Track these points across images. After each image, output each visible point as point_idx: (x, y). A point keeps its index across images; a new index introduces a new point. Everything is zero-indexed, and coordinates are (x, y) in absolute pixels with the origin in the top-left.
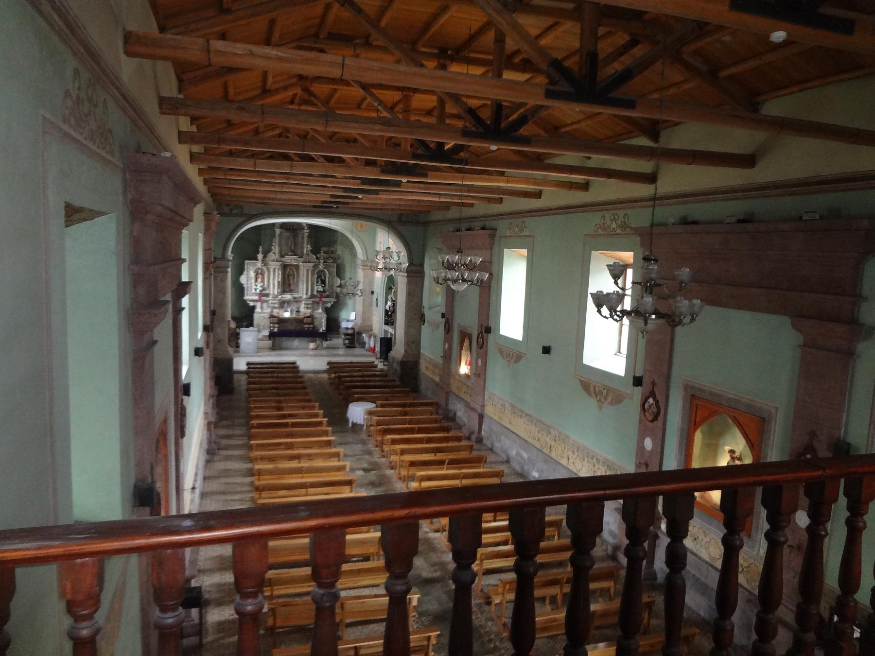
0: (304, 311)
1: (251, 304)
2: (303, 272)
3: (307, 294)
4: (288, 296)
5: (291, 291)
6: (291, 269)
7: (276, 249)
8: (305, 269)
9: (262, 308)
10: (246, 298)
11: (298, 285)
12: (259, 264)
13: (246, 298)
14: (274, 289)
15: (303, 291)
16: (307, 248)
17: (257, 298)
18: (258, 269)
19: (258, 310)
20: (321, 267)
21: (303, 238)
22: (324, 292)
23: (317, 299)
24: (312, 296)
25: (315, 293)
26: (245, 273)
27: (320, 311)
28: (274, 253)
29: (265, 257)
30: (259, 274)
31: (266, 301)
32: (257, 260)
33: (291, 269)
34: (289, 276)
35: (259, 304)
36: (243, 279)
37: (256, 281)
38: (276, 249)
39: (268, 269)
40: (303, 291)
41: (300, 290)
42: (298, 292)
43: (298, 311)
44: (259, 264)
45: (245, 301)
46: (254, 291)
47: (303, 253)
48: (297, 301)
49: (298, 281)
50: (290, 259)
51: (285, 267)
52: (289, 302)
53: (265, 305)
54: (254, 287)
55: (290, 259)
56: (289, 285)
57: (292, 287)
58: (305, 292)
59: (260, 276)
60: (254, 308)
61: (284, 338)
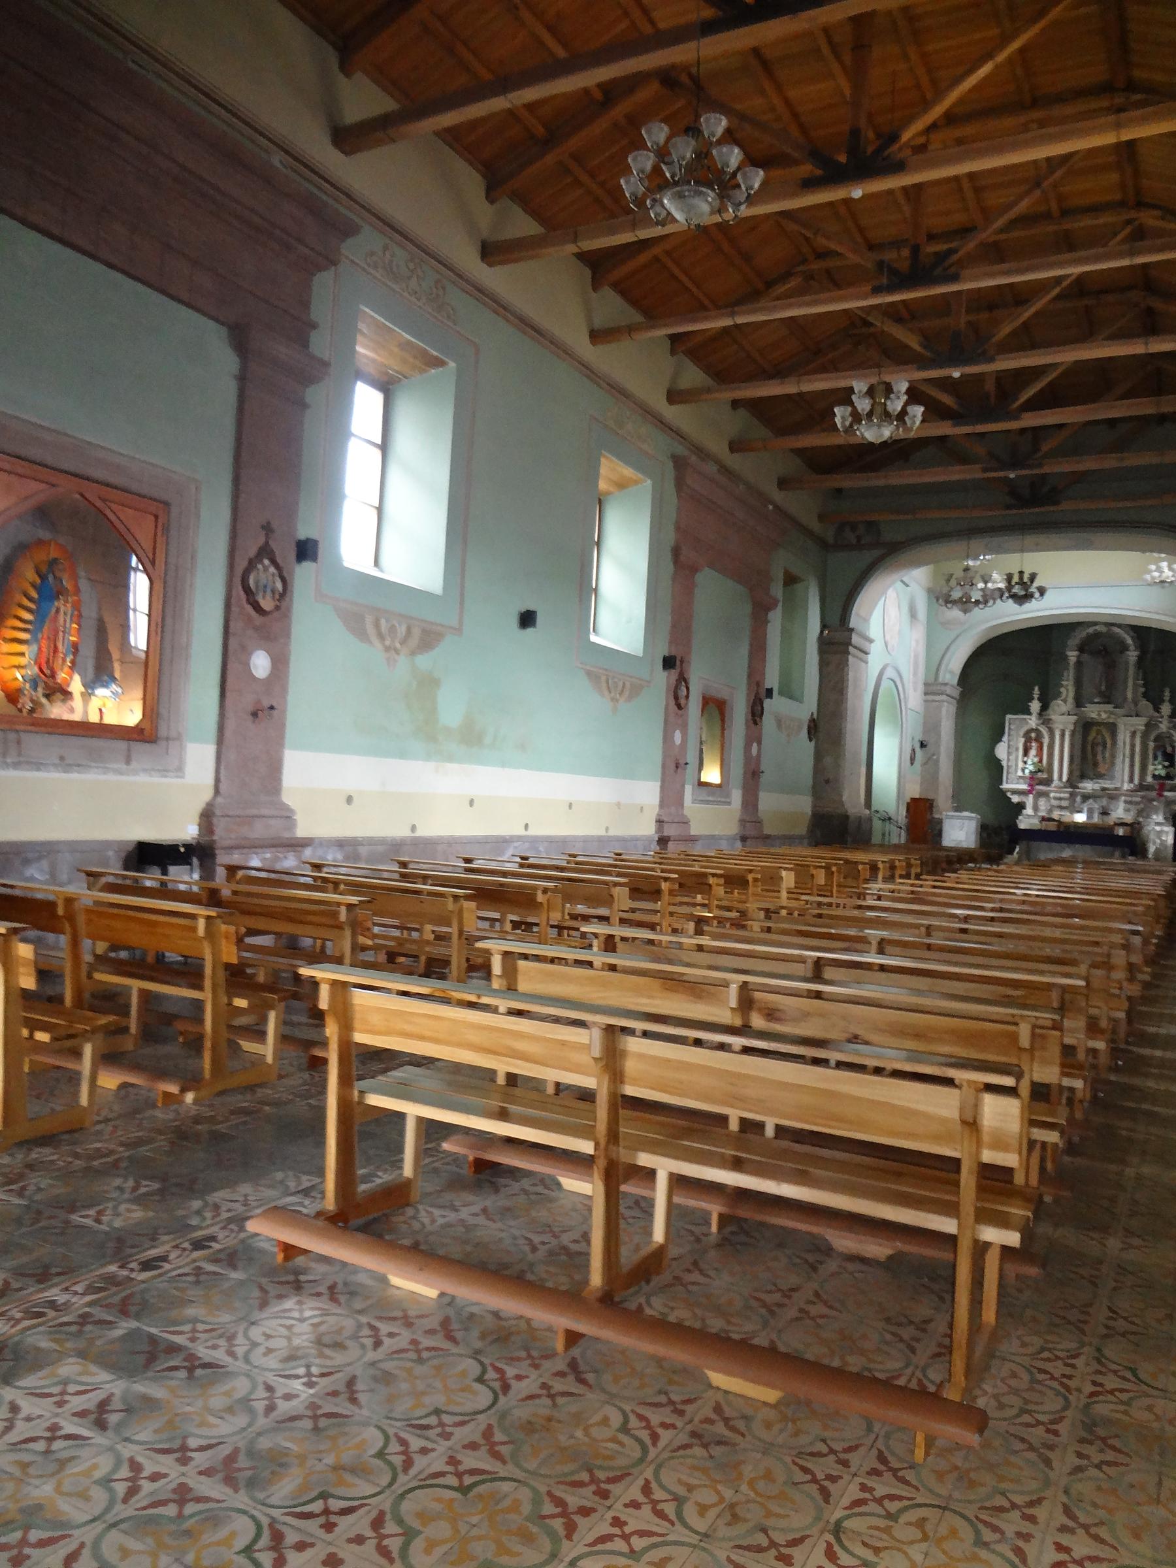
0: (1120, 812)
1: (1015, 799)
2: (1123, 737)
3: (1131, 780)
4: (1088, 786)
5: (1099, 776)
6: (1099, 732)
7: (1068, 689)
8: (1128, 731)
9: (1036, 808)
10: (1005, 786)
11: (1113, 764)
12: (1033, 721)
13: (1005, 786)
14: (1061, 769)
15: (1122, 778)
16: (1131, 687)
17: (1024, 787)
18: (1032, 730)
19: (1029, 811)
20: (1164, 726)
21: (1127, 670)
22: (1169, 777)
23: (1154, 794)
24: (1142, 787)
25: (1149, 779)
26: (1005, 738)
27: (1159, 818)
28: (1065, 701)
29: (1045, 707)
30: (1032, 739)
31: (1045, 794)
32: (1030, 714)
33: (1099, 732)
34: (1094, 745)
35: (1029, 800)
36: (1001, 751)
37: (1026, 753)
38: (1068, 689)
39: (1051, 732)
40: (1122, 778)
41: (1118, 774)
42: (1112, 778)
43: (1105, 813)
44: (1033, 721)
45: (1003, 793)
46: (1020, 773)
47: (1125, 699)
48: (1112, 795)
49: (1113, 756)
50: (1094, 711)
51: (1085, 727)
52: (1086, 797)
53: (1042, 802)
54: (1021, 765)
55: (1094, 711)
56: (1096, 764)
57: (1102, 769)
58: (1126, 778)
60: (1021, 806)
61: (1044, 844)
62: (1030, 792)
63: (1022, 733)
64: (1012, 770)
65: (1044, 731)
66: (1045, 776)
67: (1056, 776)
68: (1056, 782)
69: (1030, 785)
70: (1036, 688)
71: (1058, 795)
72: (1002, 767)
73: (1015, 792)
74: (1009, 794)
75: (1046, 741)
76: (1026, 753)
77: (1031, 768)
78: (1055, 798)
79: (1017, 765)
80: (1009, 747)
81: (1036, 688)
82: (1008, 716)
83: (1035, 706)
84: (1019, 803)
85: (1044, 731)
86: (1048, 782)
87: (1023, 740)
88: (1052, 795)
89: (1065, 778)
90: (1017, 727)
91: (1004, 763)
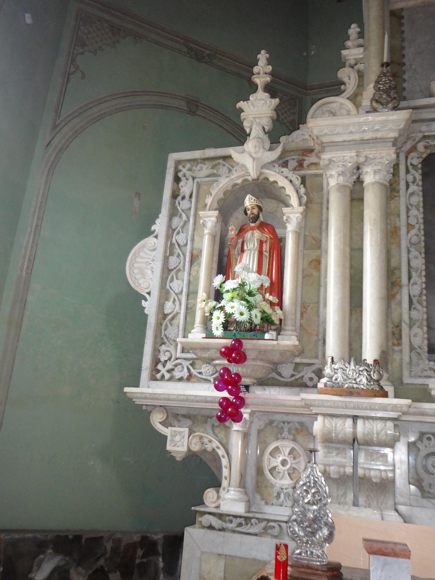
1: (179, 441)
10: (147, 389)
26: (160, 226)
30: (250, 217)
35: (233, 447)
36: (144, 267)
37: (224, 267)
44: (250, 158)
45: (139, 414)
46: (196, 336)
53: (280, 456)
54: (202, 304)
59: (253, 238)
60: (203, 472)
62: (230, 412)
63: (209, 201)
64: (173, 331)
65: (284, 181)
66: (289, 341)
67: (333, 346)
68: (337, 370)
69: (228, 381)
70: (263, 57)
71: (346, 427)
72: (143, 318)
73: (176, 414)
74: (156, 420)
75: (292, 217)
76: (224, 267)
77: (236, 308)
78: (329, 440)
79: (190, 310)
80: (170, 249)
81: (263, 57)
82: (173, 157)
83: (257, 110)
84: (191, 456)
85: (284, 181)
86: (302, 373)
87: (210, 219)
88: (318, 426)
89: (370, 353)
90: (202, 187)
91: (150, 307)
